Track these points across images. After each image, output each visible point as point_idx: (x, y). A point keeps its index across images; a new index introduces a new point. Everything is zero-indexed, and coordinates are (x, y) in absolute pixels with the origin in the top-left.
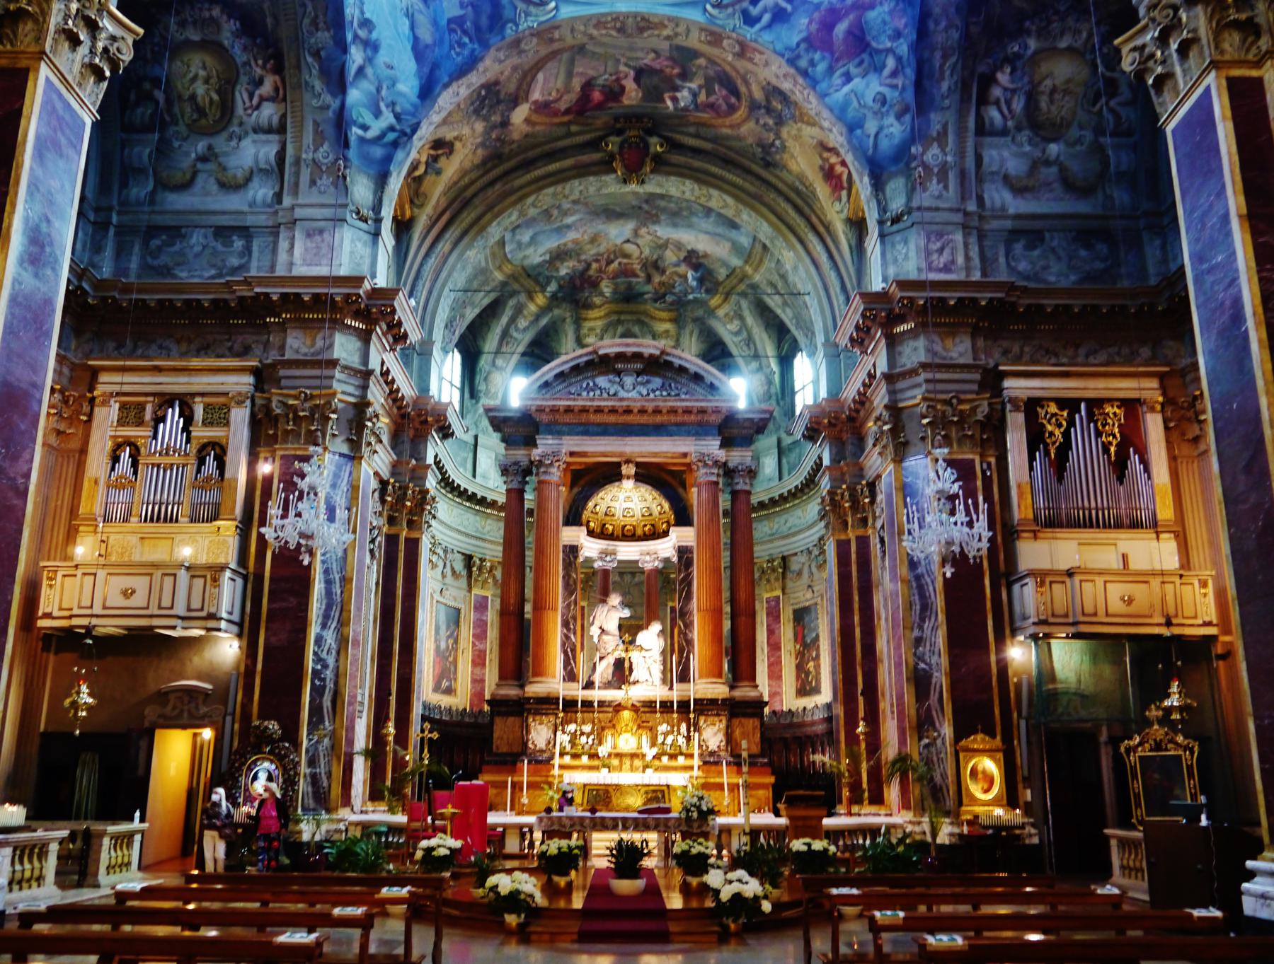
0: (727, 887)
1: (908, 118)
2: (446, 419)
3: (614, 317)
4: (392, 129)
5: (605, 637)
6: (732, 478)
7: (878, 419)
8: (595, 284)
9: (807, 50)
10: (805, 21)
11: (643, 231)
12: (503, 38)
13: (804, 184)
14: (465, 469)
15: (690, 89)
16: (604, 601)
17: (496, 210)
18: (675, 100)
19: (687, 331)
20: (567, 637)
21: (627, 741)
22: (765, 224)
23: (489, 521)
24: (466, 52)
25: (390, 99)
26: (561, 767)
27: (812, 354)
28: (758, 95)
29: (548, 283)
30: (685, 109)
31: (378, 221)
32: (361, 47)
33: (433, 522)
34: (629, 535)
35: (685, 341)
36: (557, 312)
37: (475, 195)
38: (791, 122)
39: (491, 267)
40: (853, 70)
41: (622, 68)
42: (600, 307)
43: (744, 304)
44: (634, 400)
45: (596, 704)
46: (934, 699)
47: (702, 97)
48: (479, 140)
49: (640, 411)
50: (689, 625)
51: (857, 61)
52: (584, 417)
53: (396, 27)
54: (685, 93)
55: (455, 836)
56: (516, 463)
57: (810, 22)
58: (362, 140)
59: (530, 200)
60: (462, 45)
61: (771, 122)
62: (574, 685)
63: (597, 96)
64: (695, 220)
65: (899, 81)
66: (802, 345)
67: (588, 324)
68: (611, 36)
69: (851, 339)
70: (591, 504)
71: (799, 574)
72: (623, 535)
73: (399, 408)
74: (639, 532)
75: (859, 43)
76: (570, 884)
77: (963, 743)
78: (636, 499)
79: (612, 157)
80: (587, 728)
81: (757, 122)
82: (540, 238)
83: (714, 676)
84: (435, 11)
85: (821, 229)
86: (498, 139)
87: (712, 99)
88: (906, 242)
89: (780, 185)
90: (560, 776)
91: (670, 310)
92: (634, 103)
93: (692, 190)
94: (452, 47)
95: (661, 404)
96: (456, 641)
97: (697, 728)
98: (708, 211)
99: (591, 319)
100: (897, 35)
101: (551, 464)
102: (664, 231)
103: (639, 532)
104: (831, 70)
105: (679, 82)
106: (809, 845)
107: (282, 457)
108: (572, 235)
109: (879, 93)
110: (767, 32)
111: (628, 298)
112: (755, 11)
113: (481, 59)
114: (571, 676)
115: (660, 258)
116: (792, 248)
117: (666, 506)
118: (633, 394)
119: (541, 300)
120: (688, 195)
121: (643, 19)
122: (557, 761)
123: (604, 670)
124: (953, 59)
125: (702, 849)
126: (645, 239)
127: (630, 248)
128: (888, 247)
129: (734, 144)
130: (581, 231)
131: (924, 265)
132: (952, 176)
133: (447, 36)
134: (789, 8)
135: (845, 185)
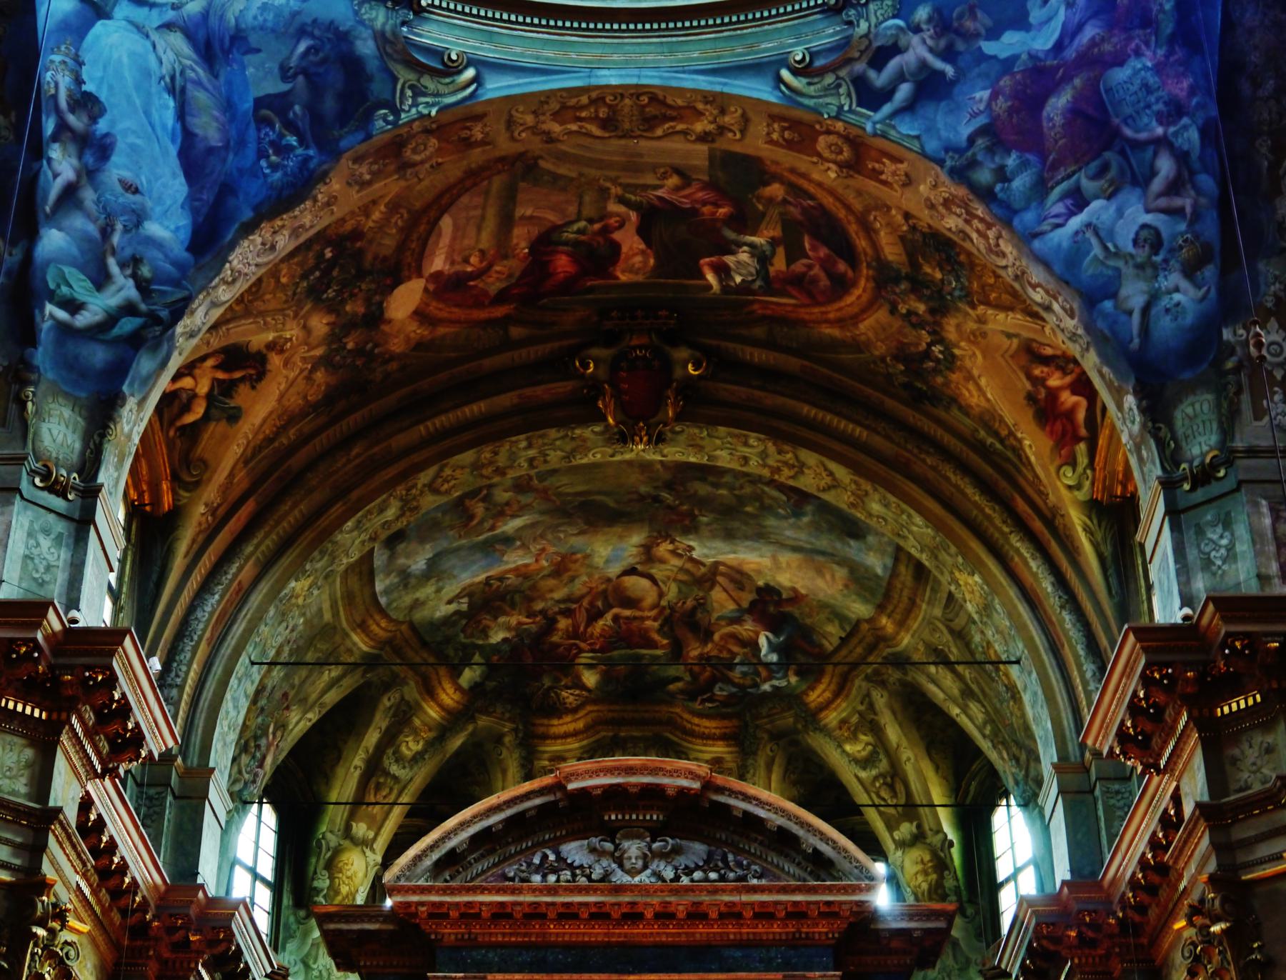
1: (1210, 272)
2: (230, 936)
3: (606, 733)
4: (128, 309)
7: (1195, 911)
8: (565, 665)
9: (990, 150)
10: (985, 94)
11: (664, 549)
12: (369, 136)
13: (996, 434)
15: (752, 245)
17: (355, 495)
18: (723, 271)
19: (761, 761)
22: (918, 520)
25: (128, 252)
27: (1029, 802)
28: (892, 252)
29: (466, 663)
30: (745, 288)
31: (91, 493)
32: (72, 148)
36: (483, 721)
37: (311, 466)
38: (963, 306)
39: (345, 624)
40: (1088, 185)
41: (614, 207)
42: (575, 710)
43: (880, 699)
47: (779, 264)
48: (319, 352)
49: (658, 916)
51: (1094, 166)
53: (147, 114)
54: (744, 256)
57: (994, 96)
58: (64, 330)
59: (424, 478)
61: (921, 308)
63: (563, 264)
64: (771, 522)
65: (1186, 202)
68: (589, 135)
69: (1122, 735)
73: (124, 912)
79: (595, 388)
81: (893, 311)
82: (448, 563)
84: (229, 83)
85: (1038, 525)
86: (359, 351)
87: (799, 266)
88: (1227, 524)
89: (948, 439)
91: (723, 717)
92: (640, 278)
93: (764, 455)
94: (262, 154)
95: (706, 898)
98: (799, 499)
99: (556, 737)
100: (1175, 111)
102: (706, 550)
104: (1041, 188)
105: (730, 234)
108: (516, 559)
109: (1145, 226)
110: (907, 118)
112: (880, 79)
113: (323, 177)
115: (702, 605)
116: (976, 566)
118: (644, 878)
119: (449, 696)
120: (754, 467)
121: (654, 98)
126: (669, 566)
127: (637, 584)
128: (1190, 535)
129: (847, 357)
130: (534, 548)
133: (252, 133)
134: (949, 70)
135: (1083, 432)
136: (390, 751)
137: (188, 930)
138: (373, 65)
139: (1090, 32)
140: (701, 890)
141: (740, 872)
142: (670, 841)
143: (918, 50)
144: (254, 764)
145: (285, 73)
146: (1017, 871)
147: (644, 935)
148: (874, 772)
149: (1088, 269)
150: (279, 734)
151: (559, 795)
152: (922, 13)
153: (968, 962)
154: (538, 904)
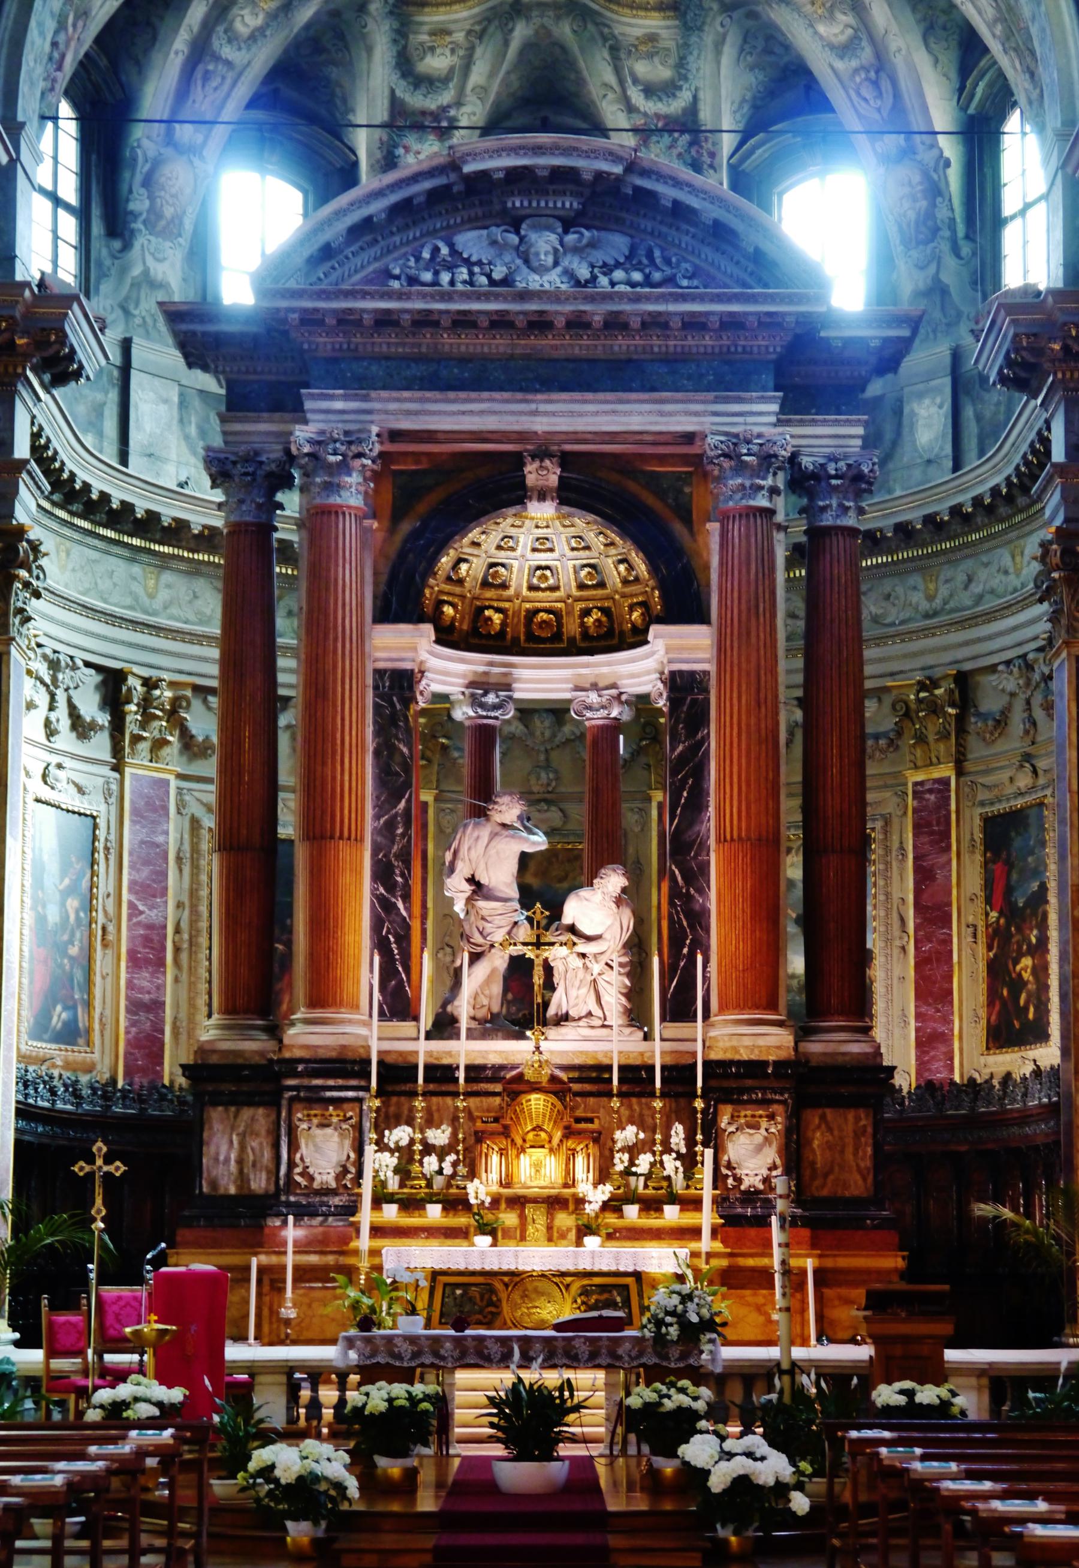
0: (723, 1464)
2: (63, 337)
6: (812, 496)
14: (100, 434)
16: (480, 813)
19: (709, 38)
21: (537, 1167)
23: (167, 577)
26: (377, 1231)
33: (35, 606)
35: (701, 66)
44: (555, 296)
45: (461, 1075)
50: (696, 876)
52: (426, 340)
55: (166, 1379)
56: (252, 458)
62: (407, 1028)
66: (1020, 96)
70: (445, 561)
71: (1001, 722)
72: (530, 637)
76: (411, 1474)
78: (562, 545)
80: (439, 1136)
83: (756, 1007)
90: (375, 1253)
95: (627, 307)
97: (714, 1138)
101: (344, 467)
103: (572, 627)
106: (910, 1394)
117: (642, 567)
118: (553, 280)
122: (366, 1216)
125: (684, 1400)
136: (220, 29)
137: (14, 332)
140: (621, 296)
141: (669, 271)
142: (587, 233)
144: (52, 67)
146: (1027, 206)
147: (555, 348)
148: (854, 63)
150: (80, 24)
151: (453, 177)
153: (959, 315)
154: (430, 312)
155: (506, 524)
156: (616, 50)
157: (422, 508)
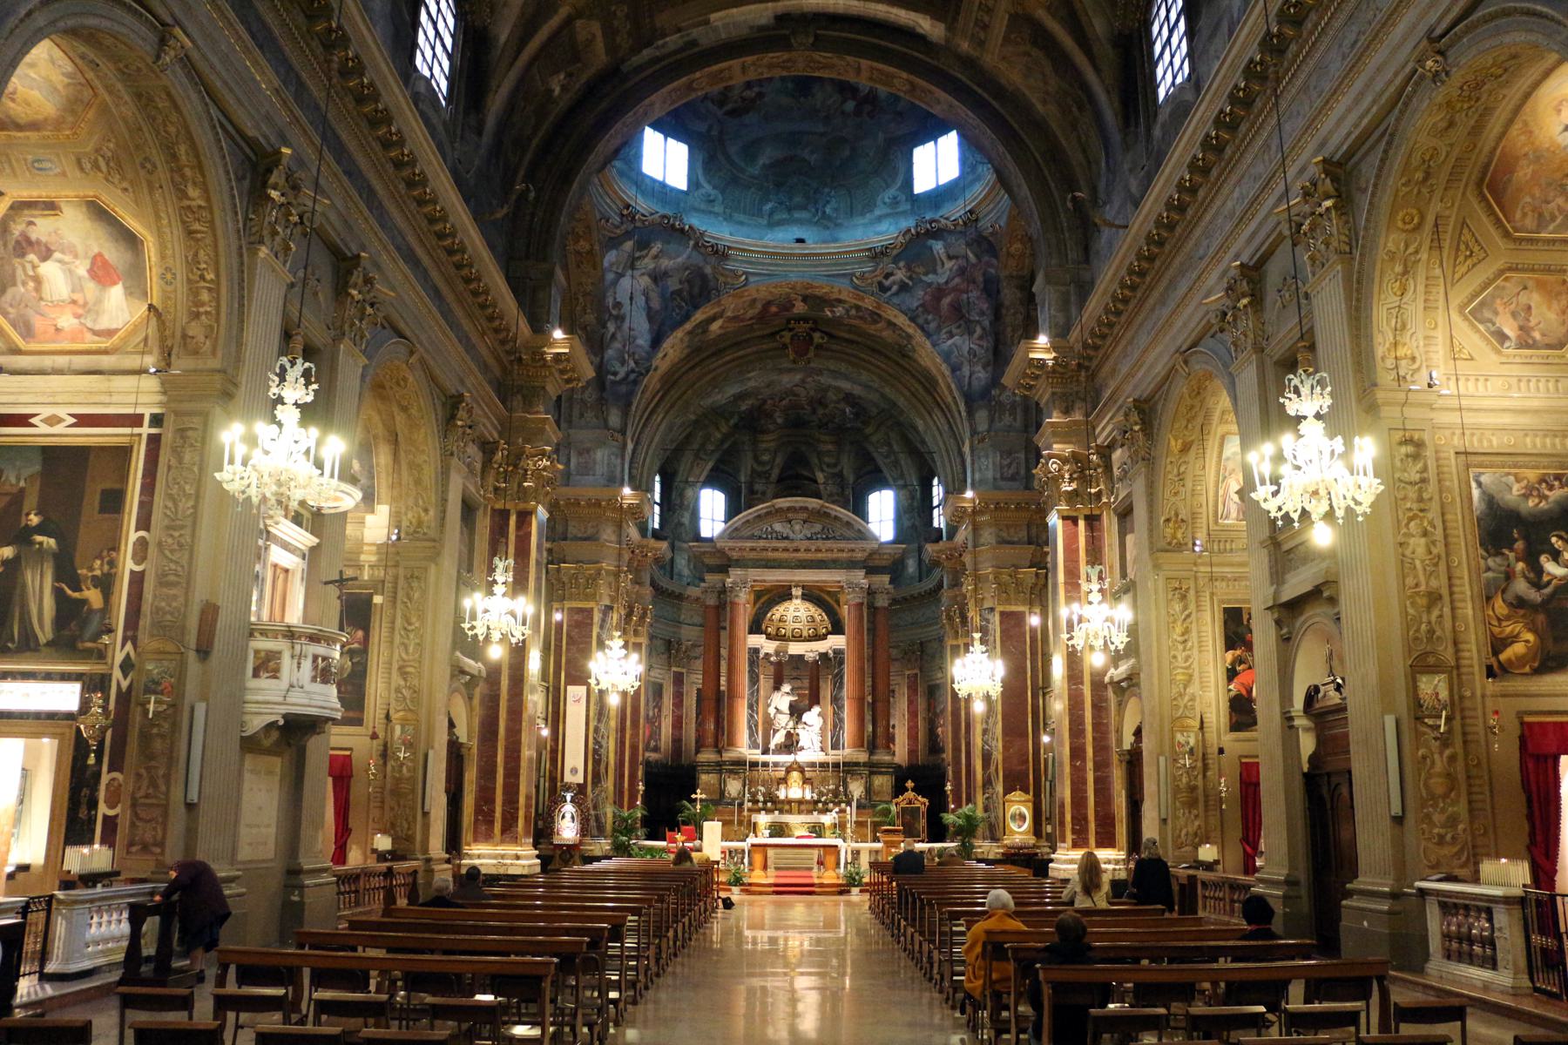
1: (990, 369)
4: (633, 371)
5: (779, 716)
8: (770, 416)
11: (809, 379)
20: (752, 716)
24: (683, 312)
34: (798, 638)
40: (954, 331)
46: (993, 768)
50: (841, 708)
58: (614, 383)
60: (680, 308)
67: (764, 445)
74: (805, 634)
75: (959, 314)
77: (1008, 797)
79: (785, 346)
96: (660, 711)
103: (805, 634)
107: (571, 609)
111: (796, 423)
112: (887, 283)
114: (754, 745)
119: (724, 429)
123: (779, 738)
124: (1020, 333)
127: (797, 390)
131: (998, 476)
132: (1019, 411)
138: (710, 277)
139: (957, 280)
143: (900, 275)
145: (681, 282)
149: (954, 360)
152: (902, 264)
155: (786, 604)
156: (820, 455)
157: (762, 600)
